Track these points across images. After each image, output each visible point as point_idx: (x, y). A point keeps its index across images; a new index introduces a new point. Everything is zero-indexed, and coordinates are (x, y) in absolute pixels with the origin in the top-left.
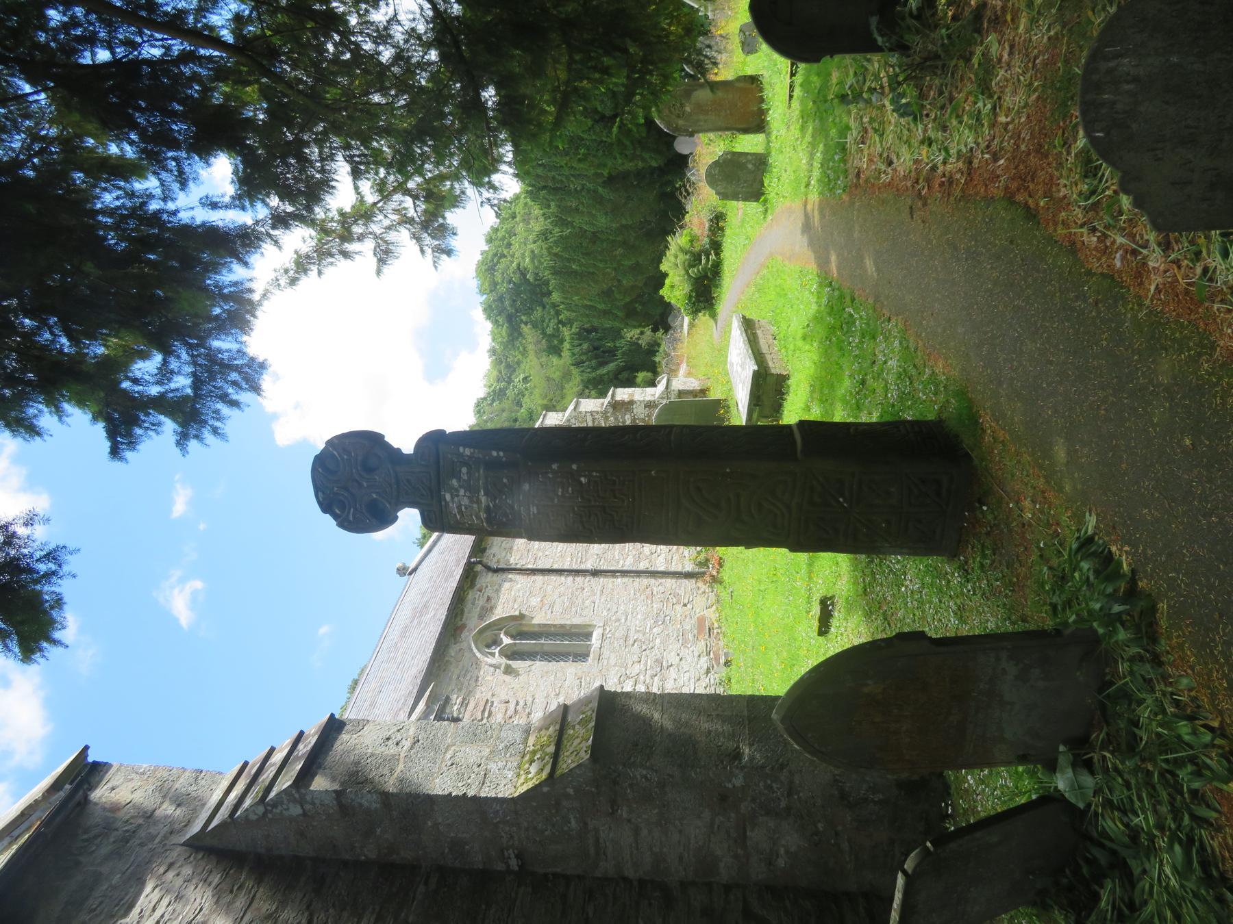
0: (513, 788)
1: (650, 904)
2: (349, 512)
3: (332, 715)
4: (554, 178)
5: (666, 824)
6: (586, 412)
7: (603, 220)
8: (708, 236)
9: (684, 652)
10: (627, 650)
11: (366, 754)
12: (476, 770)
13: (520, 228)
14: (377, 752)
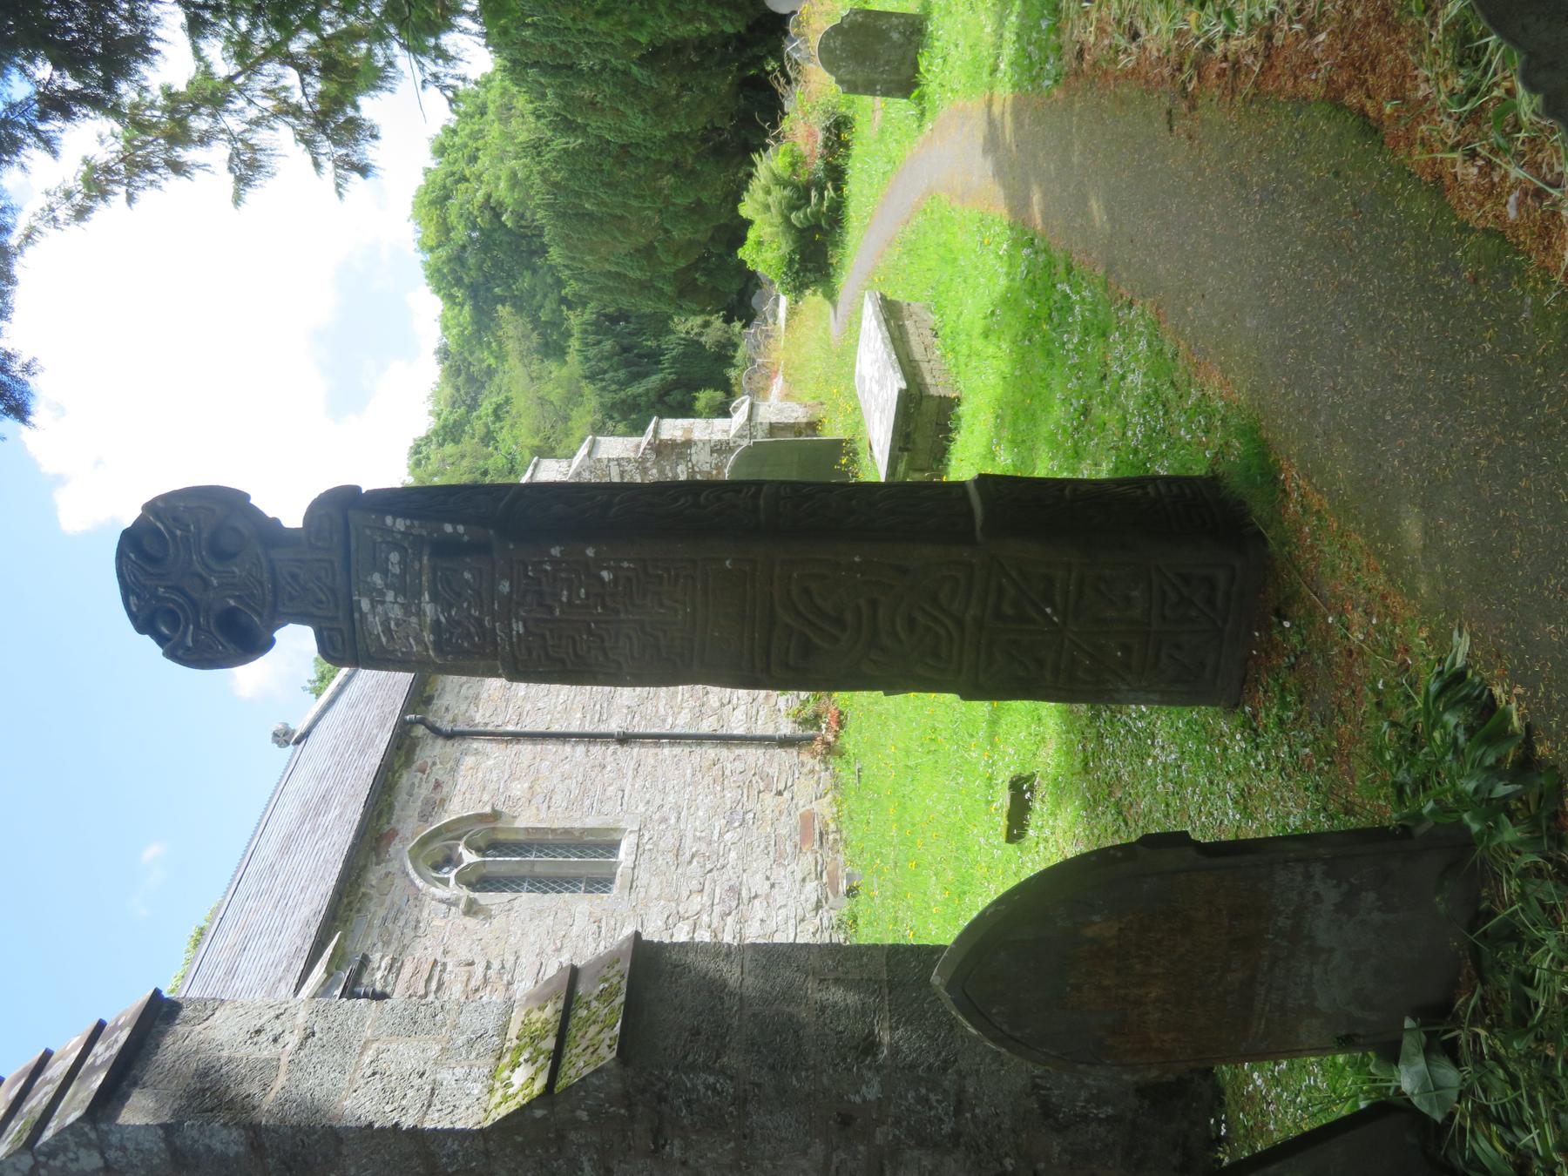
0: (482, 1111)
2: (185, 633)
3: (157, 993)
4: (553, 47)
5: (747, 1168)
6: (609, 460)
7: (639, 123)
8: (822, 157)
9: (778, 874)
10: (679, 871)
11: (219, 1059)
12: (417, 1082)
13: (494, 131)
14: (238, 1055)
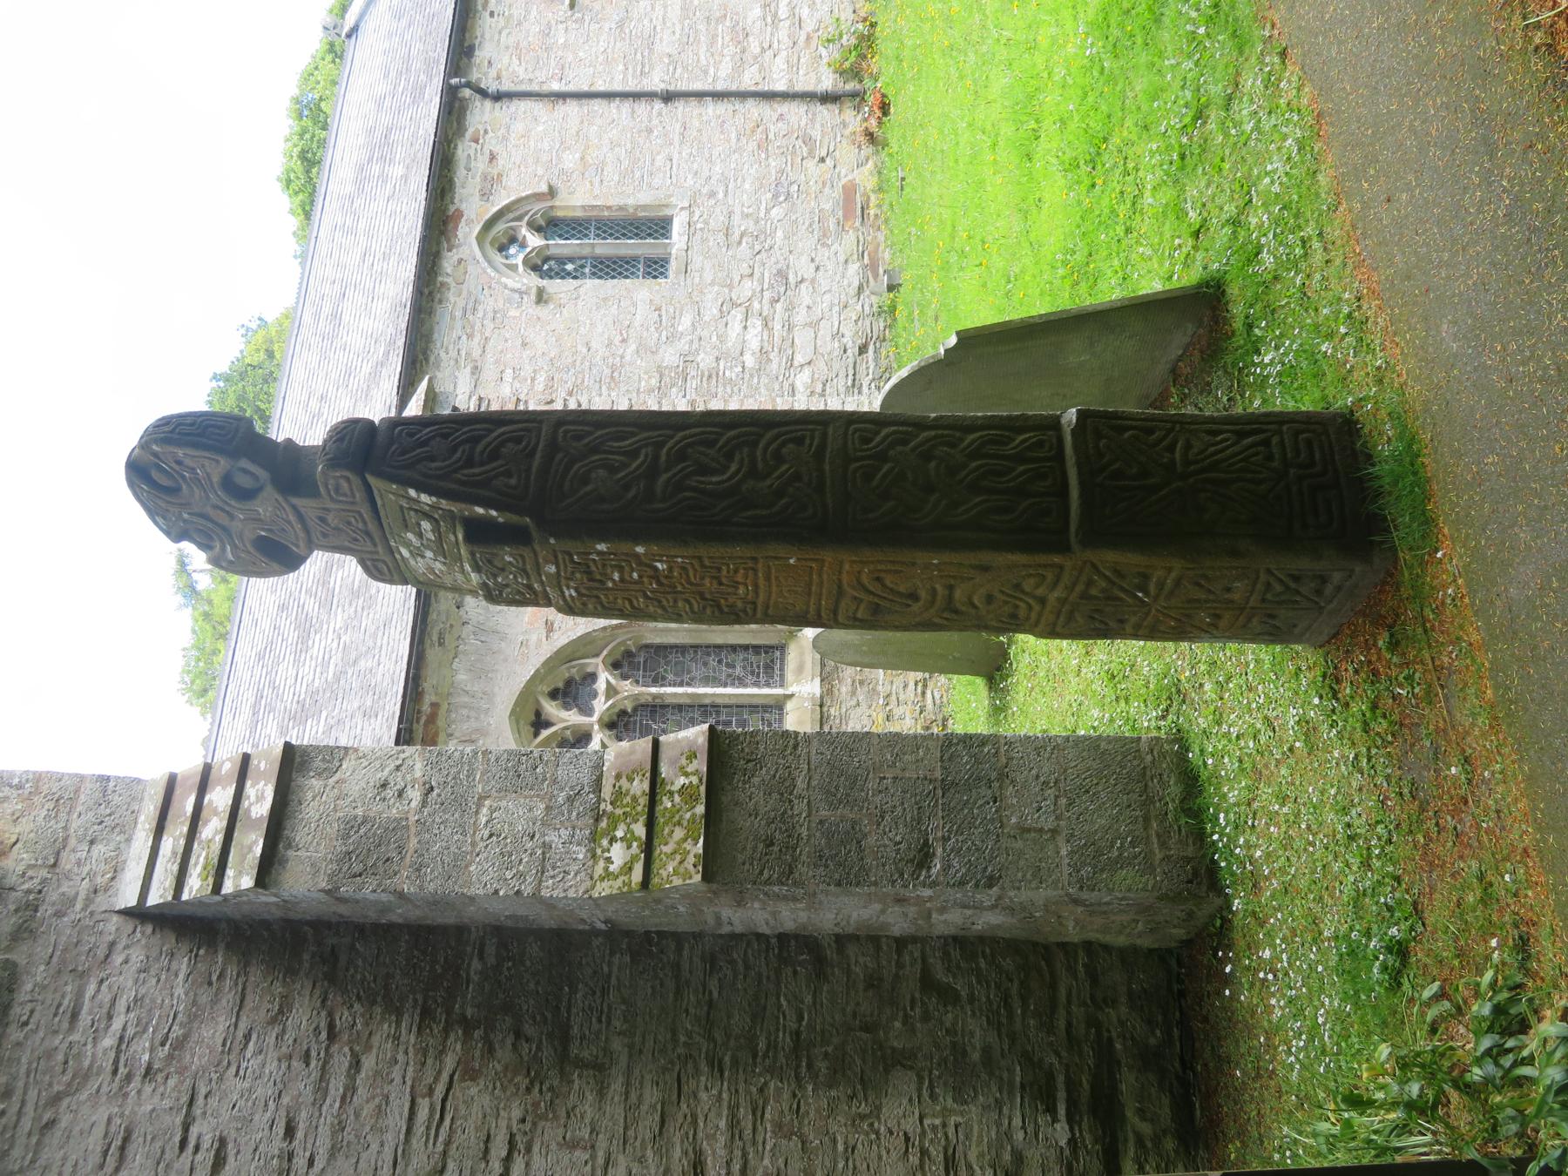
0: (588, 878)
1: (795, 972)
2: (223, 549)
9: (823, 255)
10: (730, 253)
11: (355, 817)
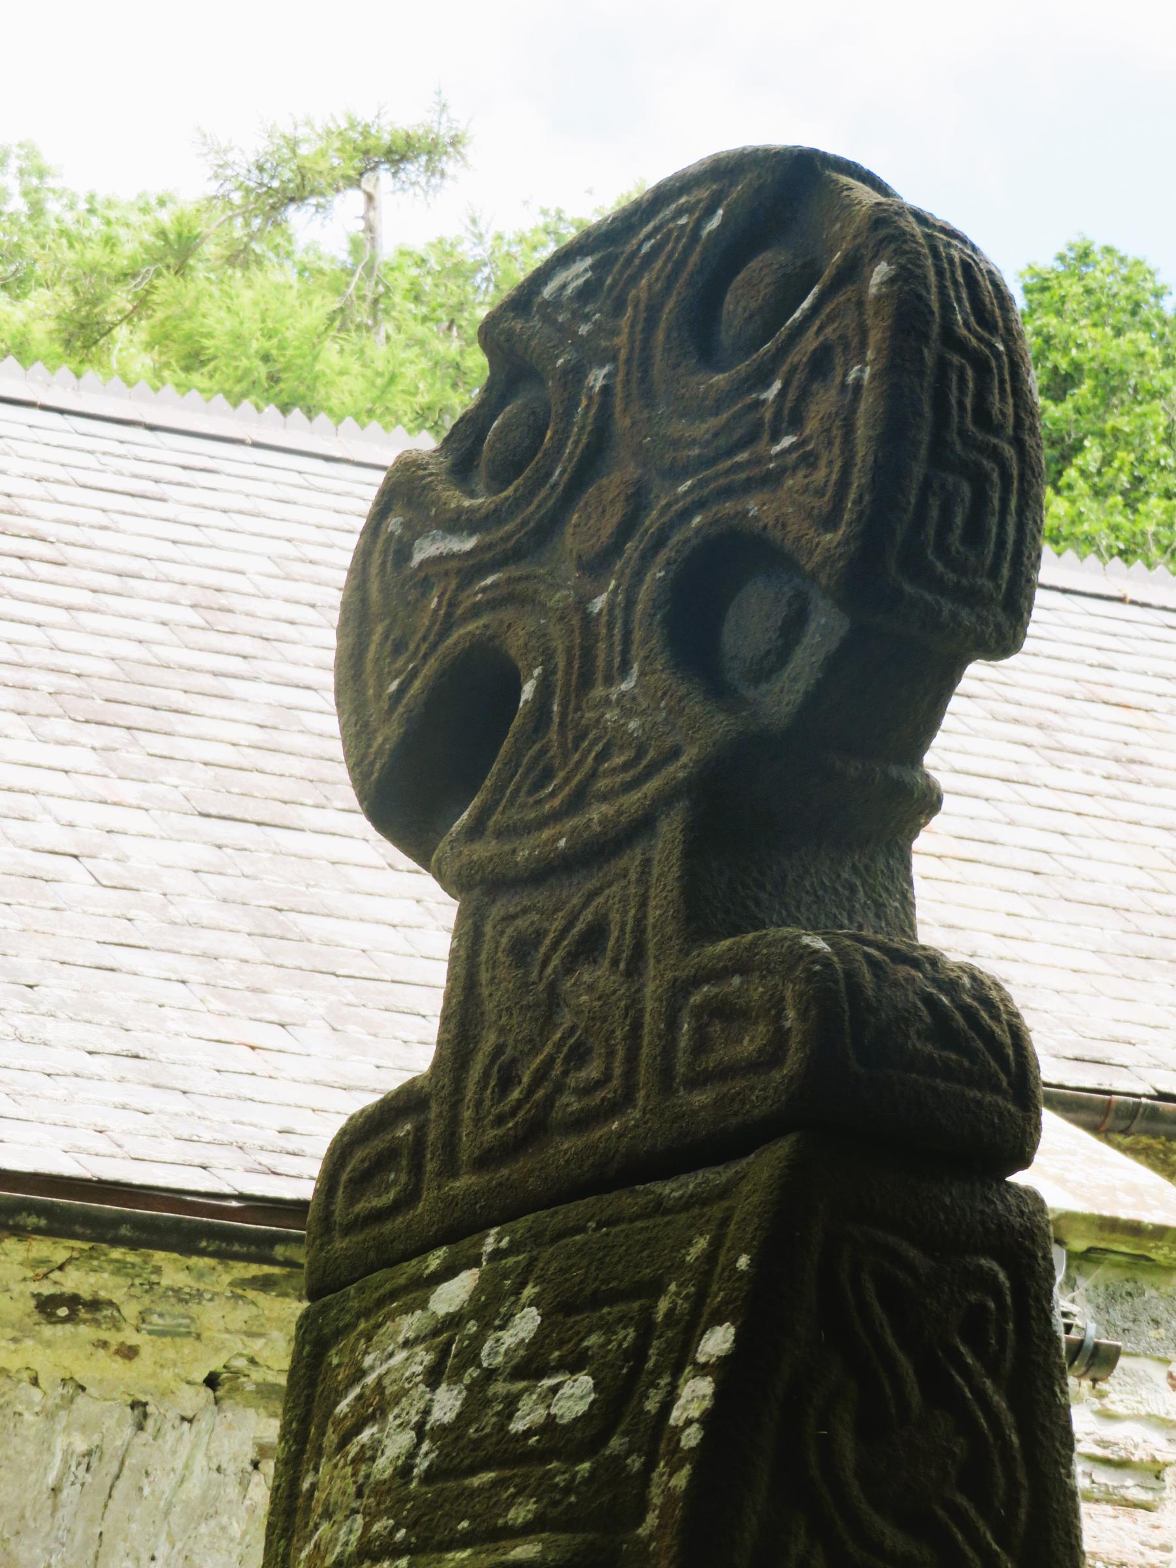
2: (457, 524)
